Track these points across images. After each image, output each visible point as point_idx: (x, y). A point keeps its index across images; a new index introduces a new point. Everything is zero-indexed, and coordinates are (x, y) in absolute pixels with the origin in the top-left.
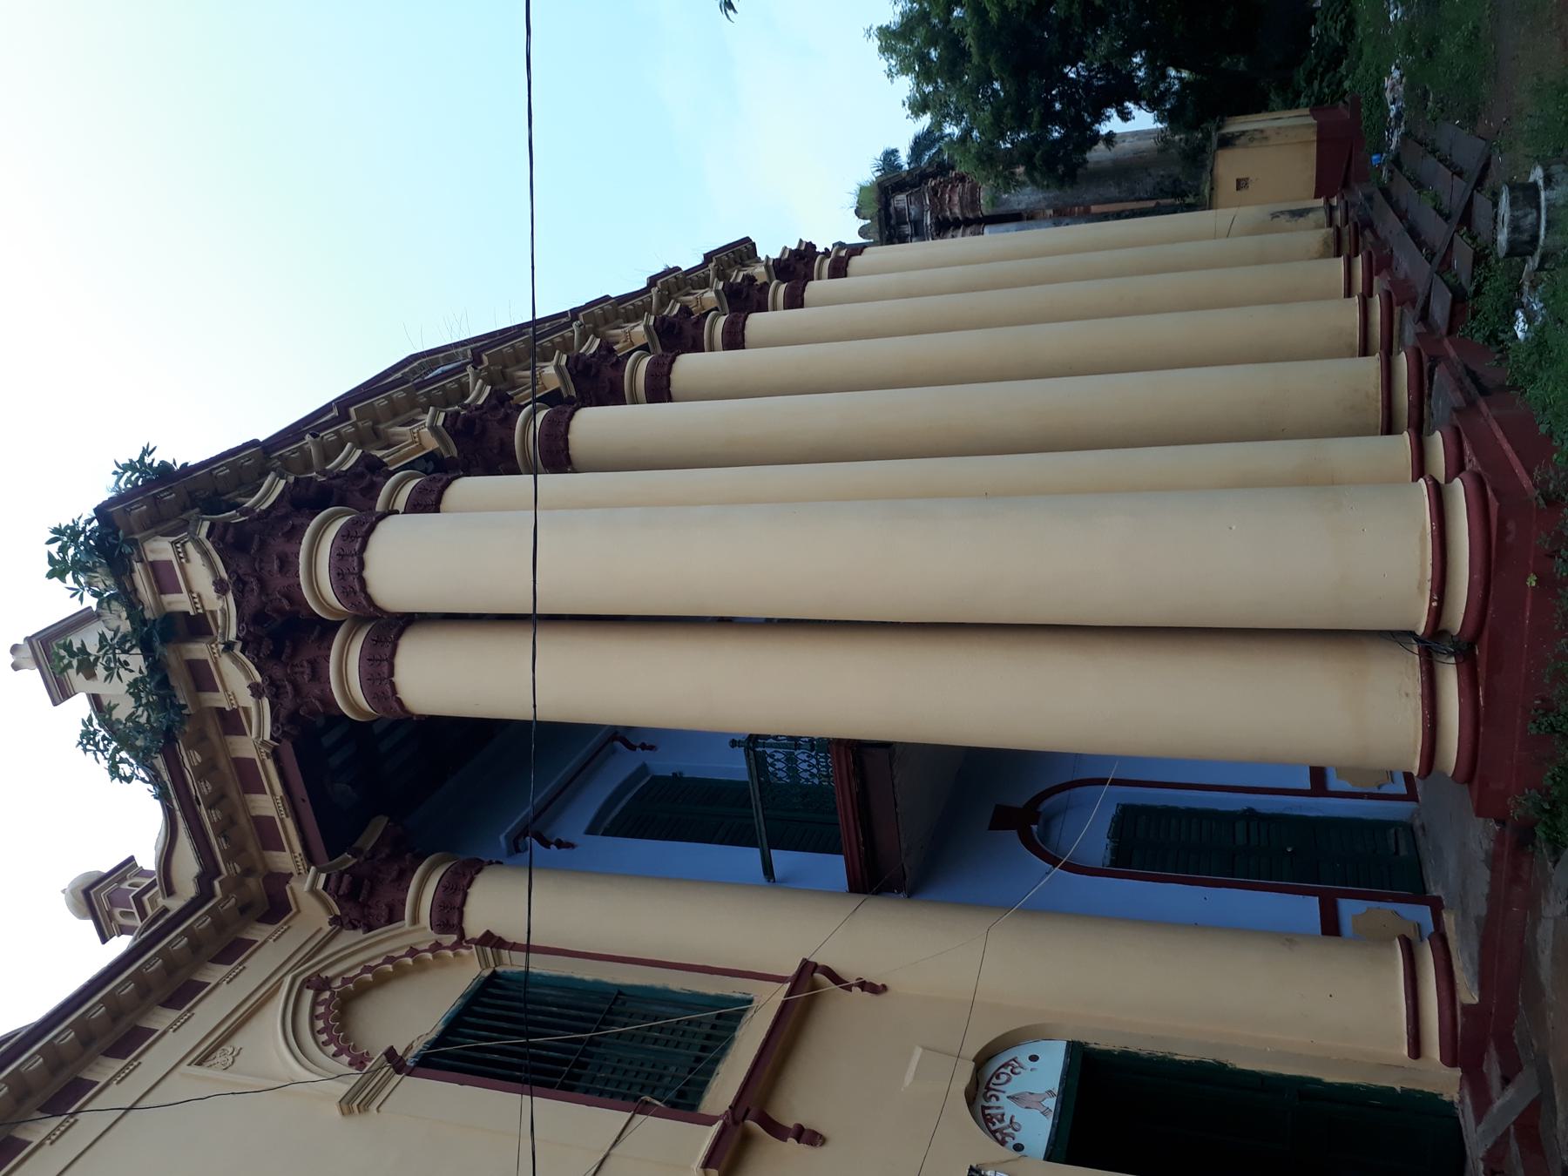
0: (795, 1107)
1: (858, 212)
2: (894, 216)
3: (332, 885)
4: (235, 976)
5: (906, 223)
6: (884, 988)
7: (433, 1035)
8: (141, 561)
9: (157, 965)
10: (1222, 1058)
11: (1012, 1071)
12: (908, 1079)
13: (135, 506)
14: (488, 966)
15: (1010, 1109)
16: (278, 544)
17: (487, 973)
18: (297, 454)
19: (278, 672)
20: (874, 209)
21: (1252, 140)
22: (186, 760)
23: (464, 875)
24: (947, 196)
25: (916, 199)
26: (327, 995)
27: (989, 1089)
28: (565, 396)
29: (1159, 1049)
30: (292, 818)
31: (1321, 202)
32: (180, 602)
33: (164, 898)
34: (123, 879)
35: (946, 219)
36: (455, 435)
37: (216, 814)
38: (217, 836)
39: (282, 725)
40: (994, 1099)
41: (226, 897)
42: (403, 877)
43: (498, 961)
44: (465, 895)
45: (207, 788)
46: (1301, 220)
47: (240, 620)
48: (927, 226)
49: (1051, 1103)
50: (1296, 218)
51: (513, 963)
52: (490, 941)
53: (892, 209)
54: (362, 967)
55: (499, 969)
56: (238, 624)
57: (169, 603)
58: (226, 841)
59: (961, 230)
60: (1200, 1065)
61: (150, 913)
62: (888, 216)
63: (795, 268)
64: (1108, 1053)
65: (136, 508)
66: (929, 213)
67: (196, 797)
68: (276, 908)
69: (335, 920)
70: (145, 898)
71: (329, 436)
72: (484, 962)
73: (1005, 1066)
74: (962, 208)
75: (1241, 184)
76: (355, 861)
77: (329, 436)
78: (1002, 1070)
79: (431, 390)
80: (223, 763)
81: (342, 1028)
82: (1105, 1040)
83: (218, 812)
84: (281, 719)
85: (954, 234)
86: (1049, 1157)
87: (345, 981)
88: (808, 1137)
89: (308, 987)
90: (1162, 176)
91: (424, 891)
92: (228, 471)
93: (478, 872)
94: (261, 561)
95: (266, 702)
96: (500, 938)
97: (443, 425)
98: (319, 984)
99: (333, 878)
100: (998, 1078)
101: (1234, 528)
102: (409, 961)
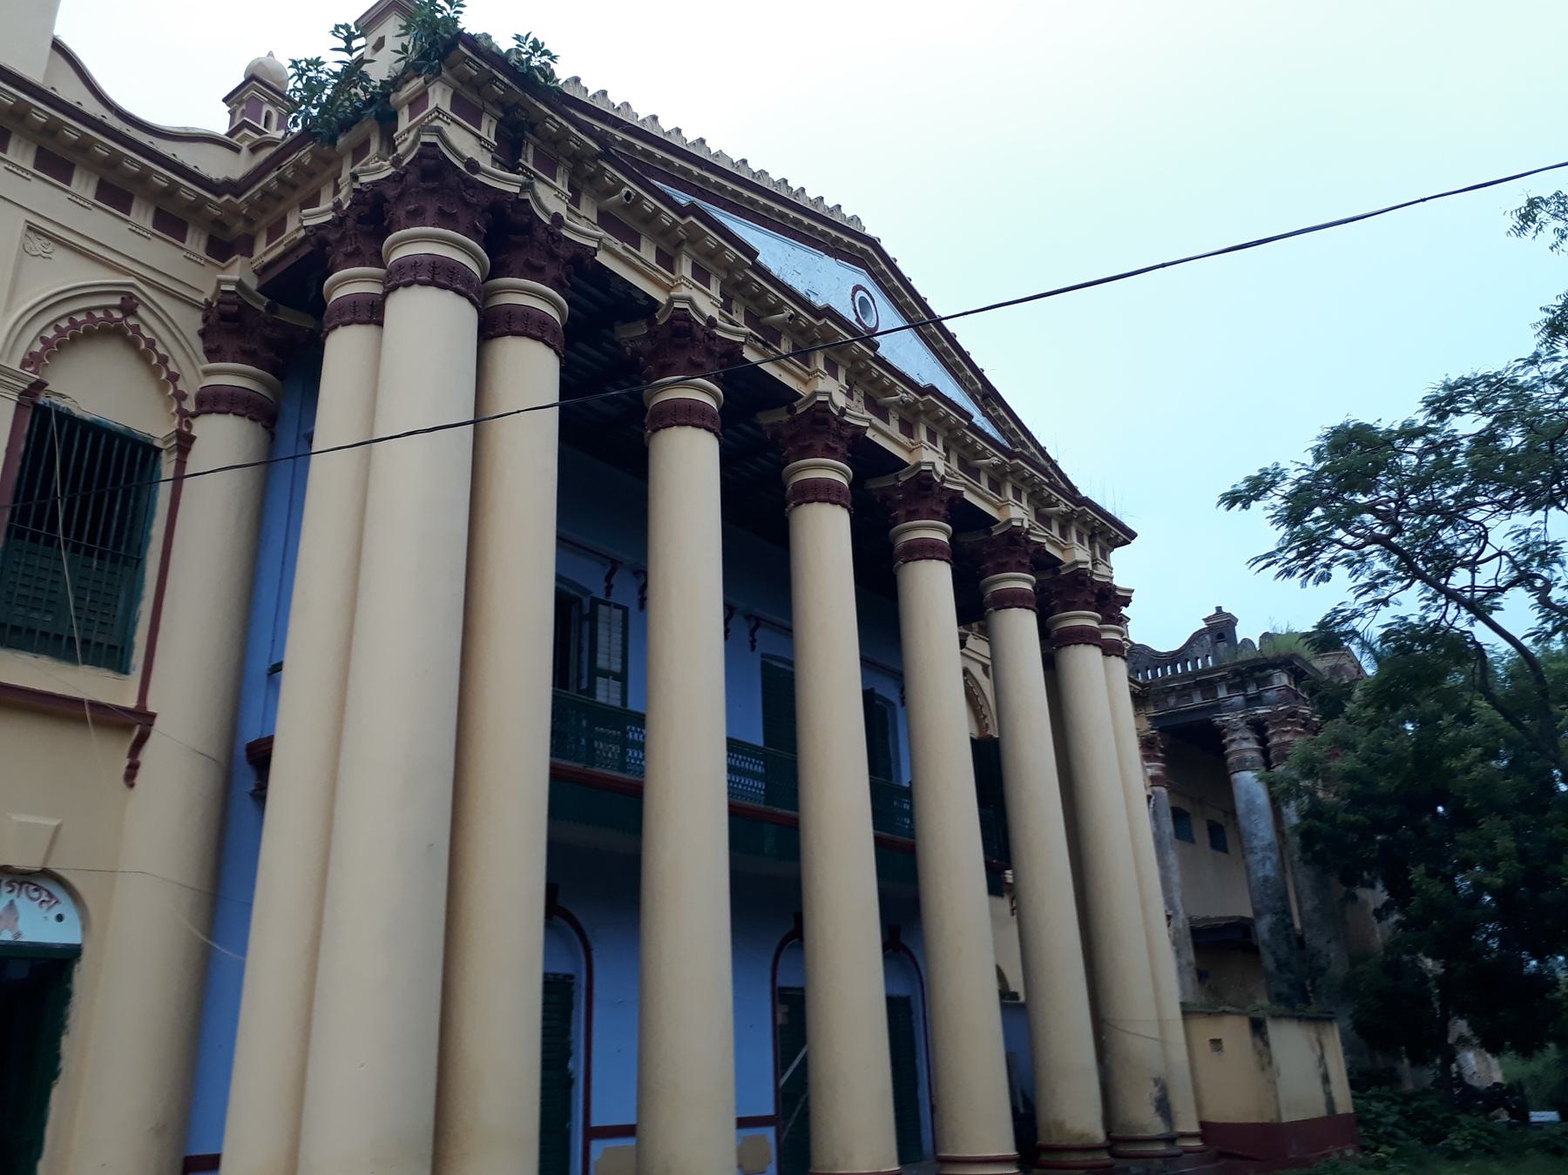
1: (1265, 636)
2: (1263, 674)
3: (227, 297)
4: (139, 234)
5: (1258, 688)
6: (132, 786)
7: (77, 413)
8: (426, 82)
9: (133, 168)
10: (62, 1078)
11: (43, 901)
12: (16, 818)
13: (473, 65)
14: (166, 442)
16: (432, 207)
17: (158, 444)
18: (611, 183)
19: (350, 223)
20: (1270, 653)
21: (1260, 1054)
22: (304, 151)
23: (247, 407)
24: (1289, 728)
25: (1283, 696)
26: (117, 315)
27: (21, 884)
28: (795, 404)
30: (284, 251)
31: (1195, 1129)
32: (404, 122)
33: (248, 146)
34: (273, 102)
35: (1266, 729)
36: (672, 319)
37: (274, 185)
38: (260, 189)
39: (314, 234)
40: (10, 889)
41: (220, 207)
42: (248, 356)
43: (169, 452)
44: (226, 413)
45: (289, 174)
46: (1151, 1109)
47: (374, 183)
48: (1254, 711)
50: (1155, 1104)
51: (167, 467)
52: (184, 442)
53: (1270, 671)
54: (153, 337)
55: (164, 454)
56: (371, 183)
57: (403, 113)
58: (261, 197)
59: (1256, 747)
60: (58, 1058)
61: (233, 140)
62: (1262, 668)
63: (1081, 591)
64: (69, 979)
65: (470, 67)
66: (1269, 711)
67: (281, 167)
68: (220, 249)
69: (208, 304)
70: (246, 131)
71: (649, 204)
72: (167, 440)
73: (50, 895)
74: (1276, 745)
75: (1216, 1044)
76: (262, 309)
77: (649, 204)
78: (44, 893)
79: (756, 281)
80: (314, 183)
81: (90, 334)
82: (82, 976)
83: (276, 187)
84: (320, 232)
85: (1251, 740)
87: (136, 329)
89: (123, 299)
90: (1328, 955)
91: (234, 376)
92: (555, 130)
93: (251, 419)
94: (418, 192)
95: (328, 217)
96: (190, 449)
97: (675, 308)
99: (233, 297)
100: (36, 890)
101: (363, 1068)
102: (164, 376)
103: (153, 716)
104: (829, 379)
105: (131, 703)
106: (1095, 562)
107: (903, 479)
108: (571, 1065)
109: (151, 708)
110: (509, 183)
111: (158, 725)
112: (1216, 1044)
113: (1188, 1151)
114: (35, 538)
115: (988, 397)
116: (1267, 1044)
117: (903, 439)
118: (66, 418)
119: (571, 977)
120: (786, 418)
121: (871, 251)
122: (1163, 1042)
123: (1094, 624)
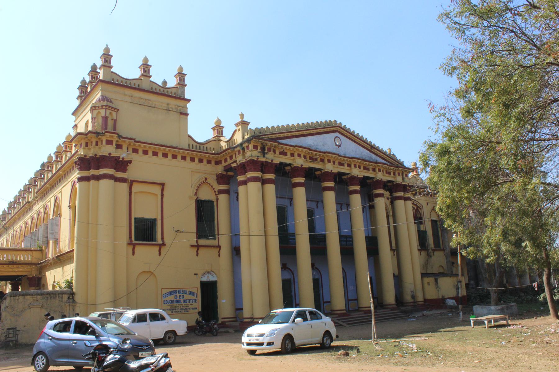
0: (201, 251)
7: (202, 199)
21: (436, 285)
49: (208, 280)
52: (217, 200)
68: (218, 163)
75: (429, 283)
82: (218, 285)
88: (197, 255)
91: (223, 187)
98: (206, 179)
104: (329, 164)
105: (217, 245)
106: (403, 179)
110: (263, 159)
111: (222, 248)
114: (200, 221)
115: (372, 148)
117: (349, 168)
120: (320, 173)
121: (338, 128)
122: (415, 284)
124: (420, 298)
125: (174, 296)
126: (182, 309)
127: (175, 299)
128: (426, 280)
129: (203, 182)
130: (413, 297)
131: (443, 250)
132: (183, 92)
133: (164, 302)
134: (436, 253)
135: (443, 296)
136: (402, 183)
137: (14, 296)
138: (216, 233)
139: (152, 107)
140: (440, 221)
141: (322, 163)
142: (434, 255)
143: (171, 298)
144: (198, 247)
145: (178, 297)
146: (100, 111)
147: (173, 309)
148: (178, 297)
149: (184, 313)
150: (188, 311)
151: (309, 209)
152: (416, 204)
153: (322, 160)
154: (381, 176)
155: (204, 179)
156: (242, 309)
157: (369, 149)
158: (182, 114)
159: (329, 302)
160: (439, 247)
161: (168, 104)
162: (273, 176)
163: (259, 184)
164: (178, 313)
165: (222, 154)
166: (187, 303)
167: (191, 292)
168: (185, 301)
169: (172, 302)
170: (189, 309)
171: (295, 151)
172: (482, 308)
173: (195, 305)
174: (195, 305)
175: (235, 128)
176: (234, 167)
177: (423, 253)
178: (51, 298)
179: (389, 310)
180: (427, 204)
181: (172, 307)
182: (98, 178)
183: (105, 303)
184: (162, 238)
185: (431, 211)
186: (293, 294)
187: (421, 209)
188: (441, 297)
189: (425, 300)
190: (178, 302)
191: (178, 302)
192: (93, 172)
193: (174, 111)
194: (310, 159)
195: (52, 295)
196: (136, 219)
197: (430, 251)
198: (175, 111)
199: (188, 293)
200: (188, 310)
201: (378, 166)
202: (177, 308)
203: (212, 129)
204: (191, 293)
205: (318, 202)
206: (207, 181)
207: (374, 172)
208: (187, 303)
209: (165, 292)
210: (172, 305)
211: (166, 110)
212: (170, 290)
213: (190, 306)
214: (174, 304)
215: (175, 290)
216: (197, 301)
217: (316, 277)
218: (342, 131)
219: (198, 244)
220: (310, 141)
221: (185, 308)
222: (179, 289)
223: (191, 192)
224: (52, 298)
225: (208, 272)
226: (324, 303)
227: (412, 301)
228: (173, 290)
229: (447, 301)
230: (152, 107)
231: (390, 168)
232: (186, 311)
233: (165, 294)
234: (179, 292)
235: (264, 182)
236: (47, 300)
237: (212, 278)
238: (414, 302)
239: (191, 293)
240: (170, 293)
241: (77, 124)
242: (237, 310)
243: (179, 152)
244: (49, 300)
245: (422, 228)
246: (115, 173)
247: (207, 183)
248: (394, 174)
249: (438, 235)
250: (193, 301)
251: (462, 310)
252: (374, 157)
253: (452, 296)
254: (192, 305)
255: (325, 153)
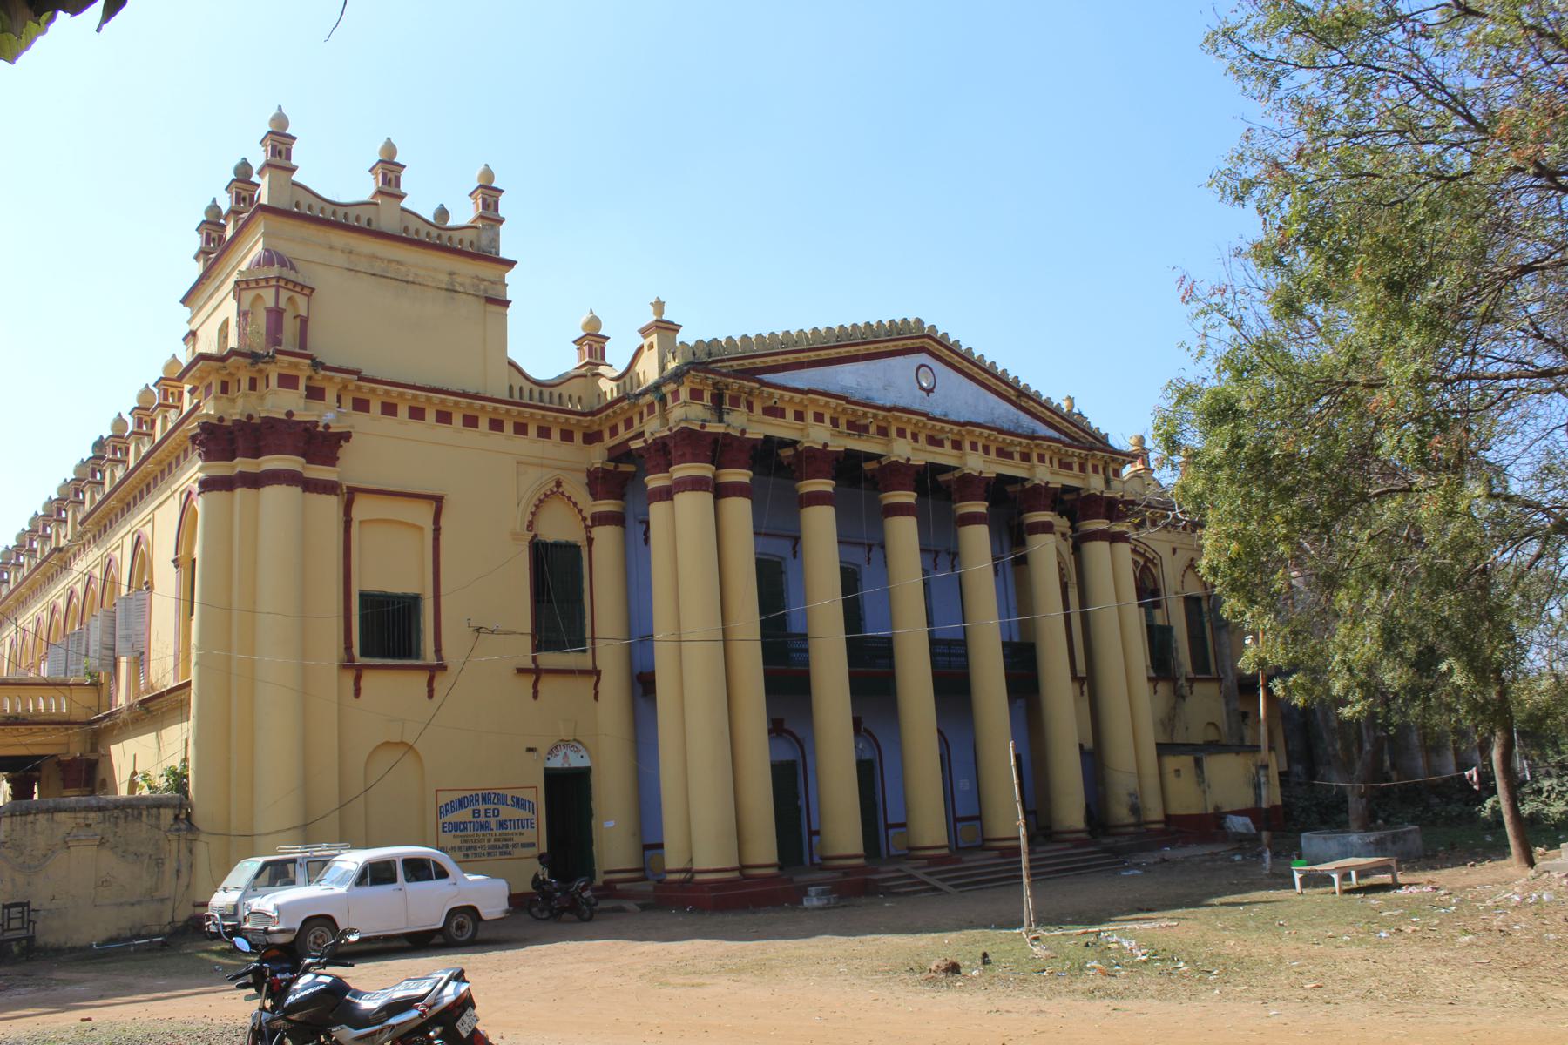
0: (547, 684)
7: (548, 541)
15: (561, 754)
21: (1198, 776)
29: (593, 796)
49: (566, 766)
52: (590, 541)
60: (591, 809)
68: (591, 438)
75: (1177, 771)
82: (594, 778)
86: (546, 769)
88: (536, 695)
91: (607, 506)
98: (559, 484)
103: (600, 671)
104: (902, 440)
105: (589, 666)
106: (1107, 482)
107: (957, 475)
108: (799, 803)
109: (599, 668)
112: (1177, 771)
113: (1149, 830)
115: (1020, 397)
116: (1202, 772)
117: (955, 452)
118: (545, 544)
119: (795, 761)
121: (927, 340)
122: (1139, 775)
123: (1105, 527)
124: (1154, 813)
125: (470, 810)
126: (494, 847)
127: (475, 820)
128: (1172, 762)
129: (551, 490)
130: (1135, 810)
131: (1218, 680)
132: (495, 240)
133: (444, 827)
134: (1197, 687)
135: (1217, 808)
136: (1105, 495)
137: (21, 815)
138: (588, 634)
139: (407, 282)
140: (1209, 600)
141: (881, 439)
142: (1191, 693)
143: (464, 815)
144: (537, 673)
145: (482, 813)
146: (262, 292)
147: (469, 848)
148: (482, 813)
149: (498, 857)
150: (510, 854)
151: (845, 565)
152: (1142, 551)
153: (883, 431)
154: (1045, 474)
155: (554, 484)
156: (660, 846)
157: (1014, 398)
158: (491, 300)
159: (903, 825)
160: (1207, 671)
161: (451, 274)
162: (747, 475)
163: (707, 497)
164: (483, 858)
165: (605, 413)
166: (508, 831)
167: (518, 799)
168: (501, 825)
169: (465, 829)
170: (514, 846)
171: (806, 406)
172: (1325, 839)
173: (529, 835)
174: (529, 835)
175: (639, 341)
176: (637, 449)
177: (1162, 687)
178: (126, 818)
179: (1068, 845)
180: (1174, 550)
181: (466, 841)
182: (255, 481)
183: (277, 832)
184: (438, 650)
185: (1185, 571)
186: (802, 802)
187: (1155, 565)
188: (1211, 810)
189: (1169, 819)
190: (484, 826)
191: (484, 826)
192: (242, 465)
193: (469, 294)
194: (848, 429)
195: (129, 810)
196: (363, 595)
197: (1182, 681)
198: (472, 292)
199: (509, 801)
200: (510, 849)
201: (1037, 445)
202: (479, 845)
203: (574, 342)
204: (518, 803)
205: (870, 547)
206: (561, 490)
207: (1026, 464)
208: (508, 831)
209: (445, 798)
210: (467, 836)
211: (447, 290)
212: (460, 795)
213: (517, 839)
214: (472, 833)
215: (474, 793)
216: (535, 825)
217: (867, 756)
218: (938, 349)
219: (537, 666)
220: (847, 378)
221: (500, 844)
222: (484, 792)
223: (516, 519)
224: (130, 818)
225: (566, 743)
226: (888, 826)
227: (1132, 820)
228: (467, 794)
229: (1228, 820)
230: (407, 282)
231: (1070, 453)
232: (505, 853)
233: (447, 804)
234: (485, 799)
235: (721, 491)
236: (116, 824)
237: (576, 761)
238: (1138, 825)
239: (518, 803)
240: (460, 804)
241: (195, 329)
242: (647, 847)
243: (483, 407)
244: (121, 822)
245: (1159, 618)
246: (304, 468)
247: (563, 494)
248: (1082, 468)
249: (1204, 639)
250: (523, 823)
251: (1269, 846)
252: (1026, 420)
253: (1242, 807)
254: (521, 834)
255: (890, 409)
